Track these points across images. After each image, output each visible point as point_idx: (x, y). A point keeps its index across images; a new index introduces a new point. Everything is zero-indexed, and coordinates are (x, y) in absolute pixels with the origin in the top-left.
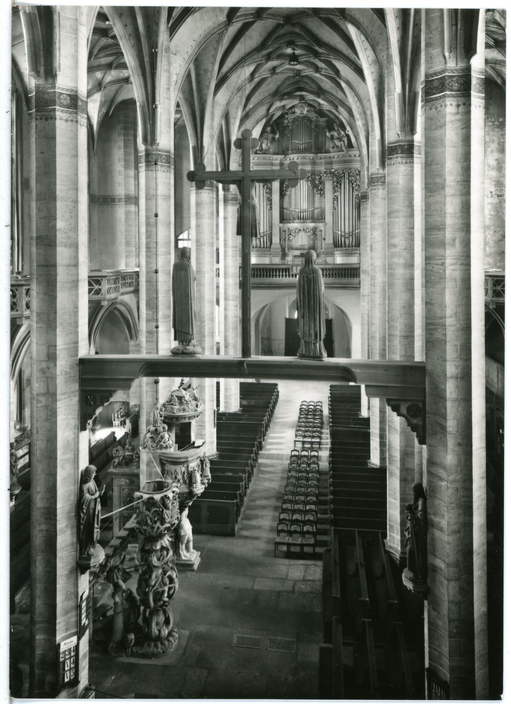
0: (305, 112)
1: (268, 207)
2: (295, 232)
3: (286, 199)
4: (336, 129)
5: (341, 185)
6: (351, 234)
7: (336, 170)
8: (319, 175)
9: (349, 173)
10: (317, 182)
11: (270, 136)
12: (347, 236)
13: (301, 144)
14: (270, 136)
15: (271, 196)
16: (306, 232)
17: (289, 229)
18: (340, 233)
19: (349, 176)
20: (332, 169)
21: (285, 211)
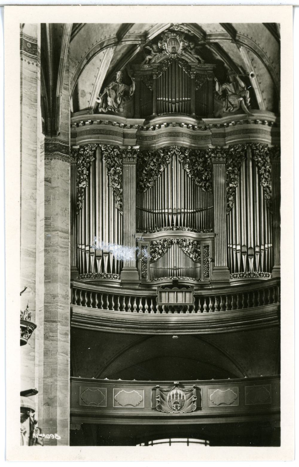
0: (180, 50)
1: (117, 205)
2: (163, 246)
3: (148, 197)
5: (239, 170)
6: (257, 249)
7: (230, 147)
8: (204, 156)
9: (253, 150)
11: (122, 87)
12: (250, 252)
13: (172, 102)
14: (122, 87)
15: (122, 187)
16: (182, 246)
17: (152, 243)
18: (239, 248)
19: (253, 155)
20: (225, 145)
21: (146, 214)
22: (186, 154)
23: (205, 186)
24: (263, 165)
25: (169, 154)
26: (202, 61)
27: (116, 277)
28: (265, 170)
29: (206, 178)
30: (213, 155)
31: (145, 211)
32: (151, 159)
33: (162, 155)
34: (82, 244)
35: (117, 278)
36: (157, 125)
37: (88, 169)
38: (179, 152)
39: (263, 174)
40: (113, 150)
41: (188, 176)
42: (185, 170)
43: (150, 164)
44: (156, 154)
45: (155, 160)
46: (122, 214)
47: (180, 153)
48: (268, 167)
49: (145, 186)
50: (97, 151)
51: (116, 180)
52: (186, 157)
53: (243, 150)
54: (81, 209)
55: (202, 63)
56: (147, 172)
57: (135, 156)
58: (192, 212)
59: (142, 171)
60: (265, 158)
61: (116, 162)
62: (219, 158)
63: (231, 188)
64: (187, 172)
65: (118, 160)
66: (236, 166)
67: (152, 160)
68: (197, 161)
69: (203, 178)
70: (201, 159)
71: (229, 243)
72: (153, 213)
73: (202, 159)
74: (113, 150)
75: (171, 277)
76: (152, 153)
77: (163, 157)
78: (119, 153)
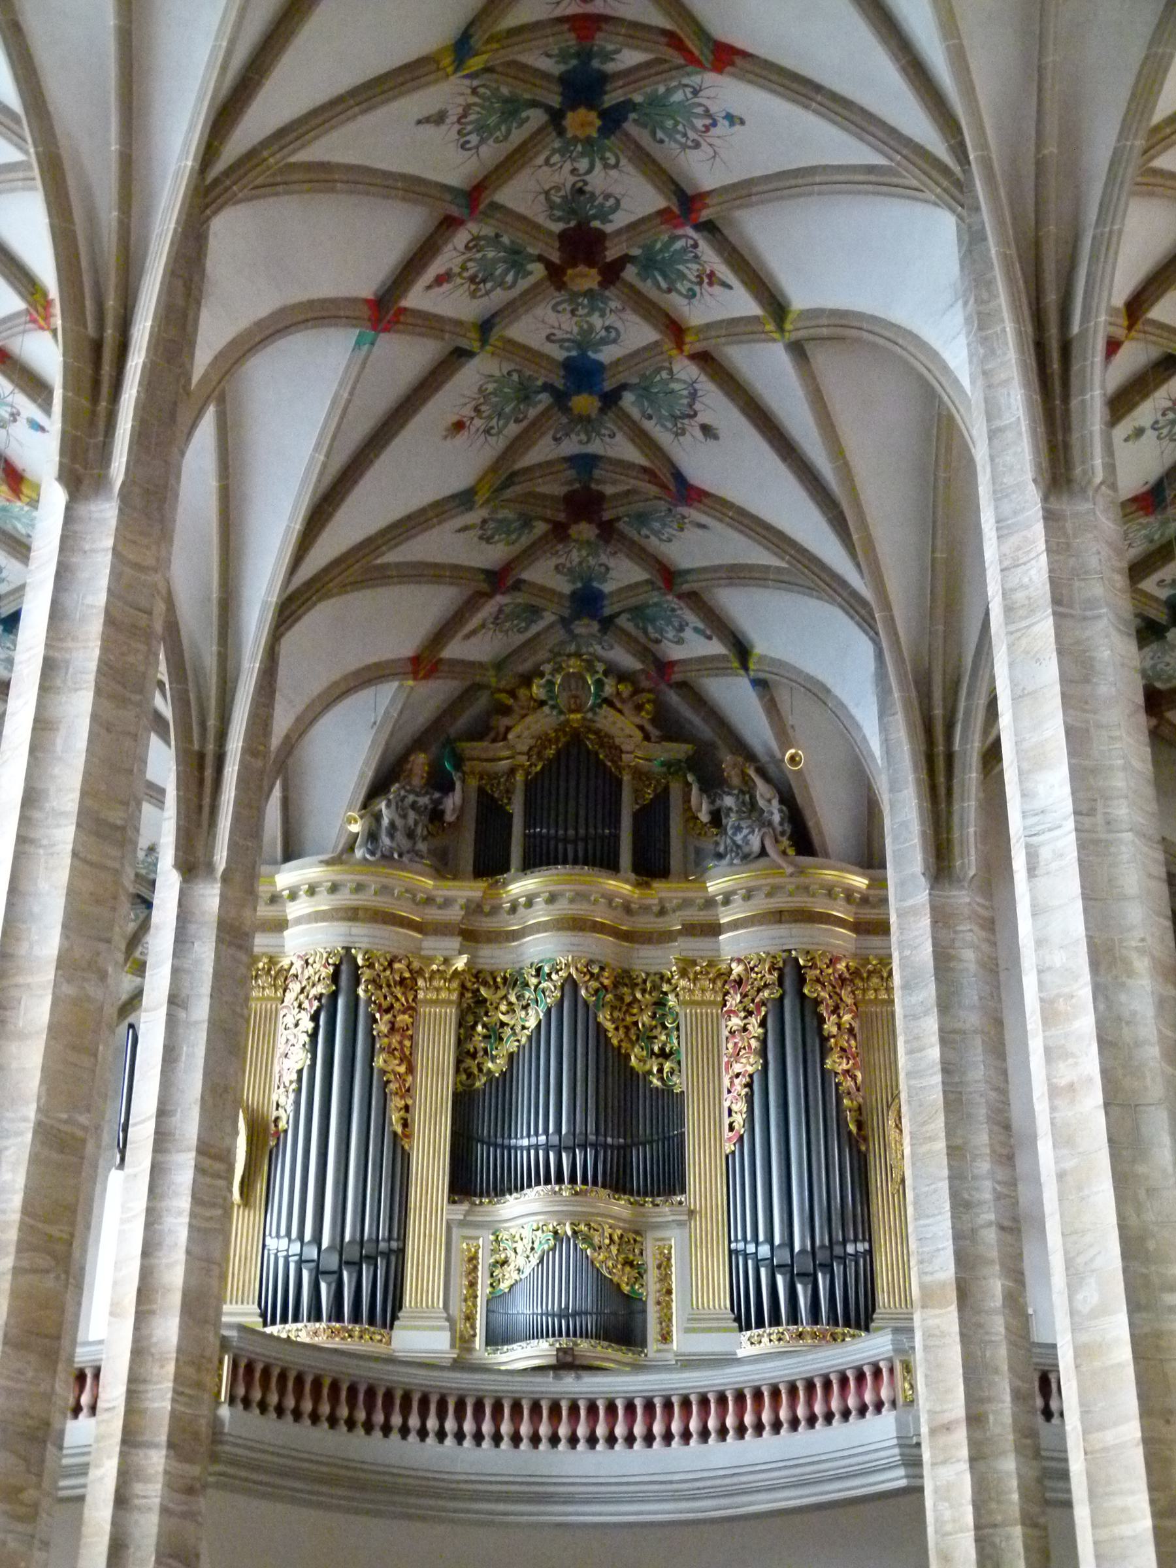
4: (736, 781)
6: (821, 1256)
8: (656, 987)
10: (645, 1018)
22: (606, 982)
23: (660, 1071)
24: (835, 1010)
25: (554, 977)
26: (654, 732)
27: (379, 1337)
28: (839, 1026)
29: (662, 1049)
30: (682, 983)
31: (483, 1143)
32: (502, 993)
33: (534, 981)
34: (278, 1236)
35: (381, 1341)
36: (523, 900)
37: (315, 1018)
38: (585, 974)
39: (834, 1036)
40: (390, 964)
41: (607, 1039)
42: (599, 1025)
43: (497, 1008)
44: (515, 981)
45: (513, 999)
46: (406, 1147)
47: (588, 977)
48: (847, 1018)
49: (480, 1070)
50: (344, 968)
51: (395, 1049)
52: (605, 987)
53: (772, 968)
54: (286, 1131)
55: (653, 739)
56: (488, 1029)
57: (455, 984)
58: (619, 1147)
59: (474, 1027)
60: (838, 990)
61: (397, 999)
62: (703, 991)
63: (738, 1075)
64: (606, 1031)
65: (404, 994)
66: (750, 1013)
67: (505, 997)
68: (635, 1000)
69: (656, 1049)
70: (647, 996)
71: (732, 1238)
72: (503, 1147)
73: (650, 993)
74: (390, 964)
75: (551, 1340)
76: (505, 979)
77: (536, 987)
78: (407, 975)
